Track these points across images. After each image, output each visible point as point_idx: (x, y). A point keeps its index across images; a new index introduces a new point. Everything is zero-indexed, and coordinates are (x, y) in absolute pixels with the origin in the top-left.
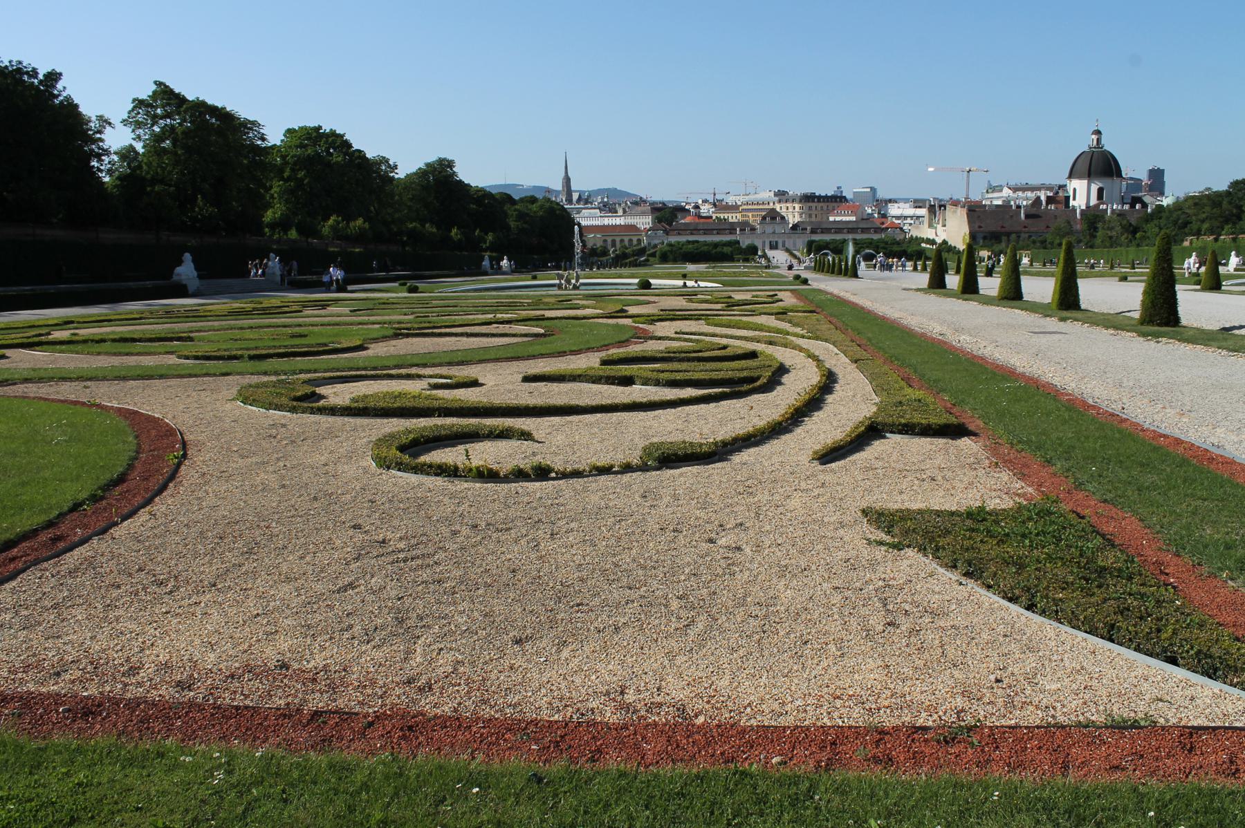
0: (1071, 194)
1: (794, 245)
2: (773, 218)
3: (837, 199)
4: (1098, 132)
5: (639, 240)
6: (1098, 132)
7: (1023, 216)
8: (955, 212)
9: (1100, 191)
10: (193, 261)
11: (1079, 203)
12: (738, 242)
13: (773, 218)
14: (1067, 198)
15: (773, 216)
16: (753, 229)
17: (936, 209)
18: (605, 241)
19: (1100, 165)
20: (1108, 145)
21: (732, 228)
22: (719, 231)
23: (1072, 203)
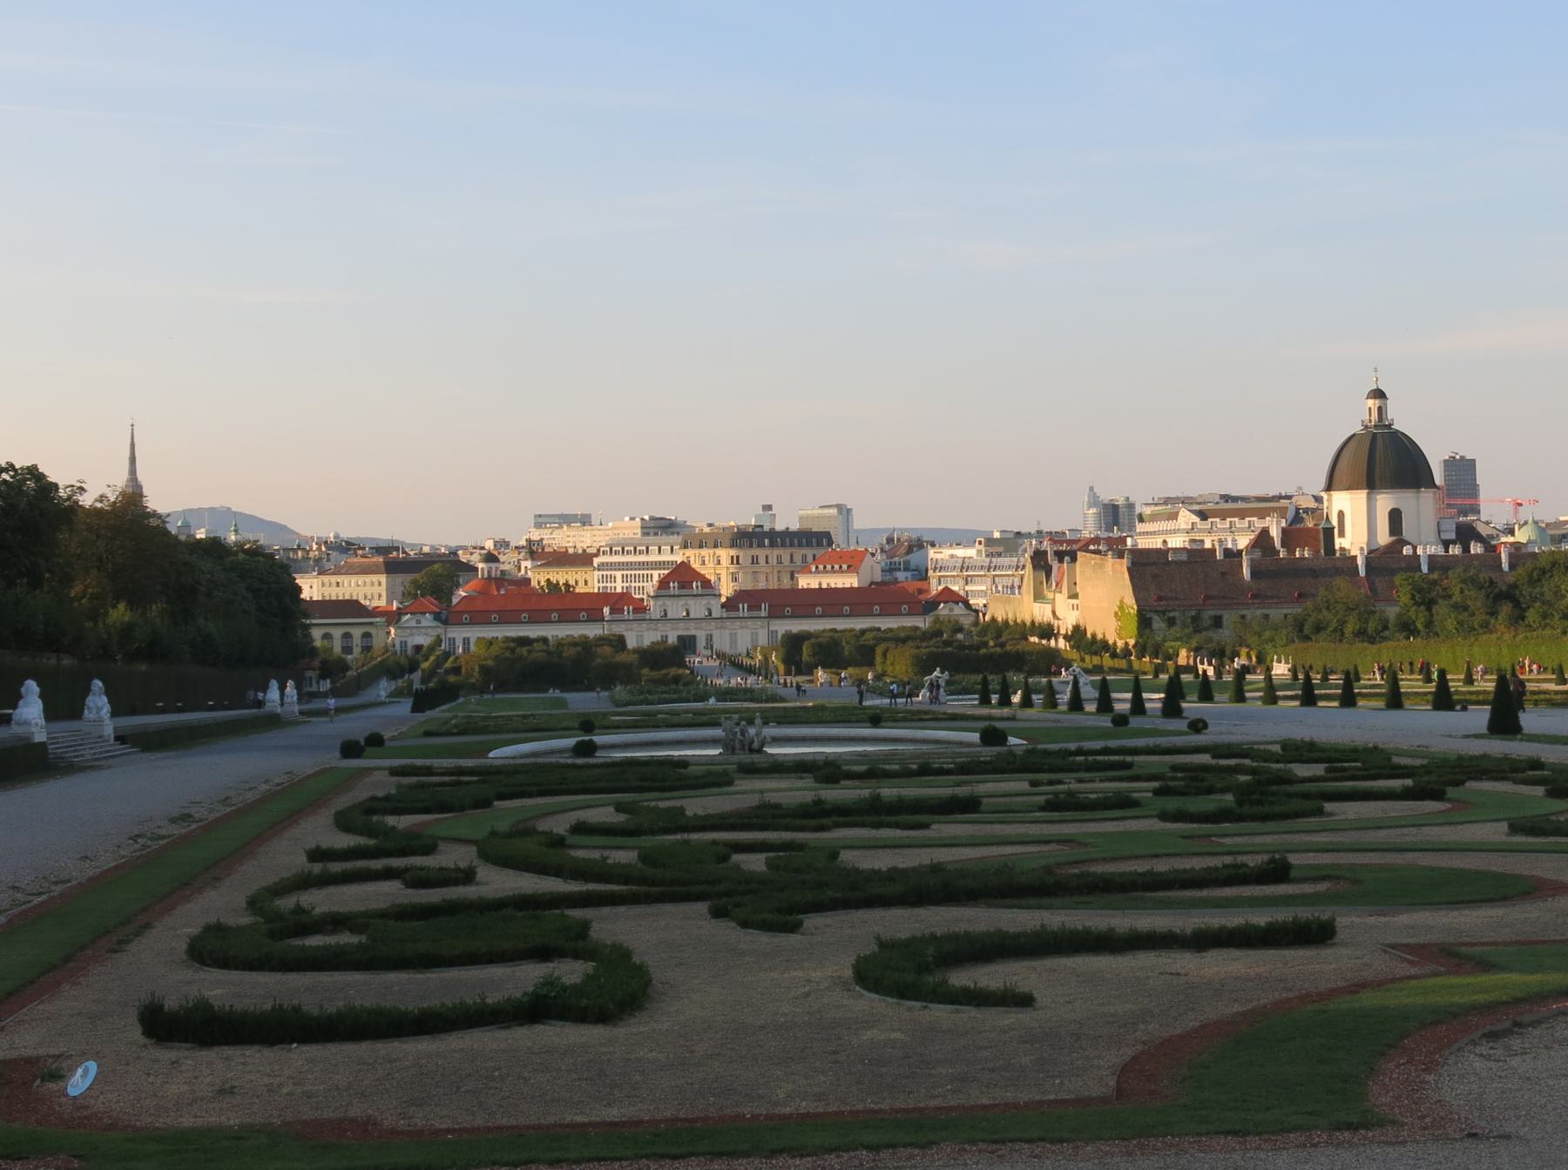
0: (1335, 522)
1: (733, 641)
3: (811, 541)
4: (1379, 394)
5: (367, 635)
6: (1379, 394)
7: (1246, 572)
8: (1101, 566)
9: (1395, 517)
10: (41, 696)
11: (1353, 541)
12: (620, 642)
14: (1329, 532)
15: (682, 578)
16: (640, 608)
17: (1052, 557)
19: (1386, 459)
20: (1402, 421)
21: (591, 607)
22: (568, 616)
23: (1339, 542)
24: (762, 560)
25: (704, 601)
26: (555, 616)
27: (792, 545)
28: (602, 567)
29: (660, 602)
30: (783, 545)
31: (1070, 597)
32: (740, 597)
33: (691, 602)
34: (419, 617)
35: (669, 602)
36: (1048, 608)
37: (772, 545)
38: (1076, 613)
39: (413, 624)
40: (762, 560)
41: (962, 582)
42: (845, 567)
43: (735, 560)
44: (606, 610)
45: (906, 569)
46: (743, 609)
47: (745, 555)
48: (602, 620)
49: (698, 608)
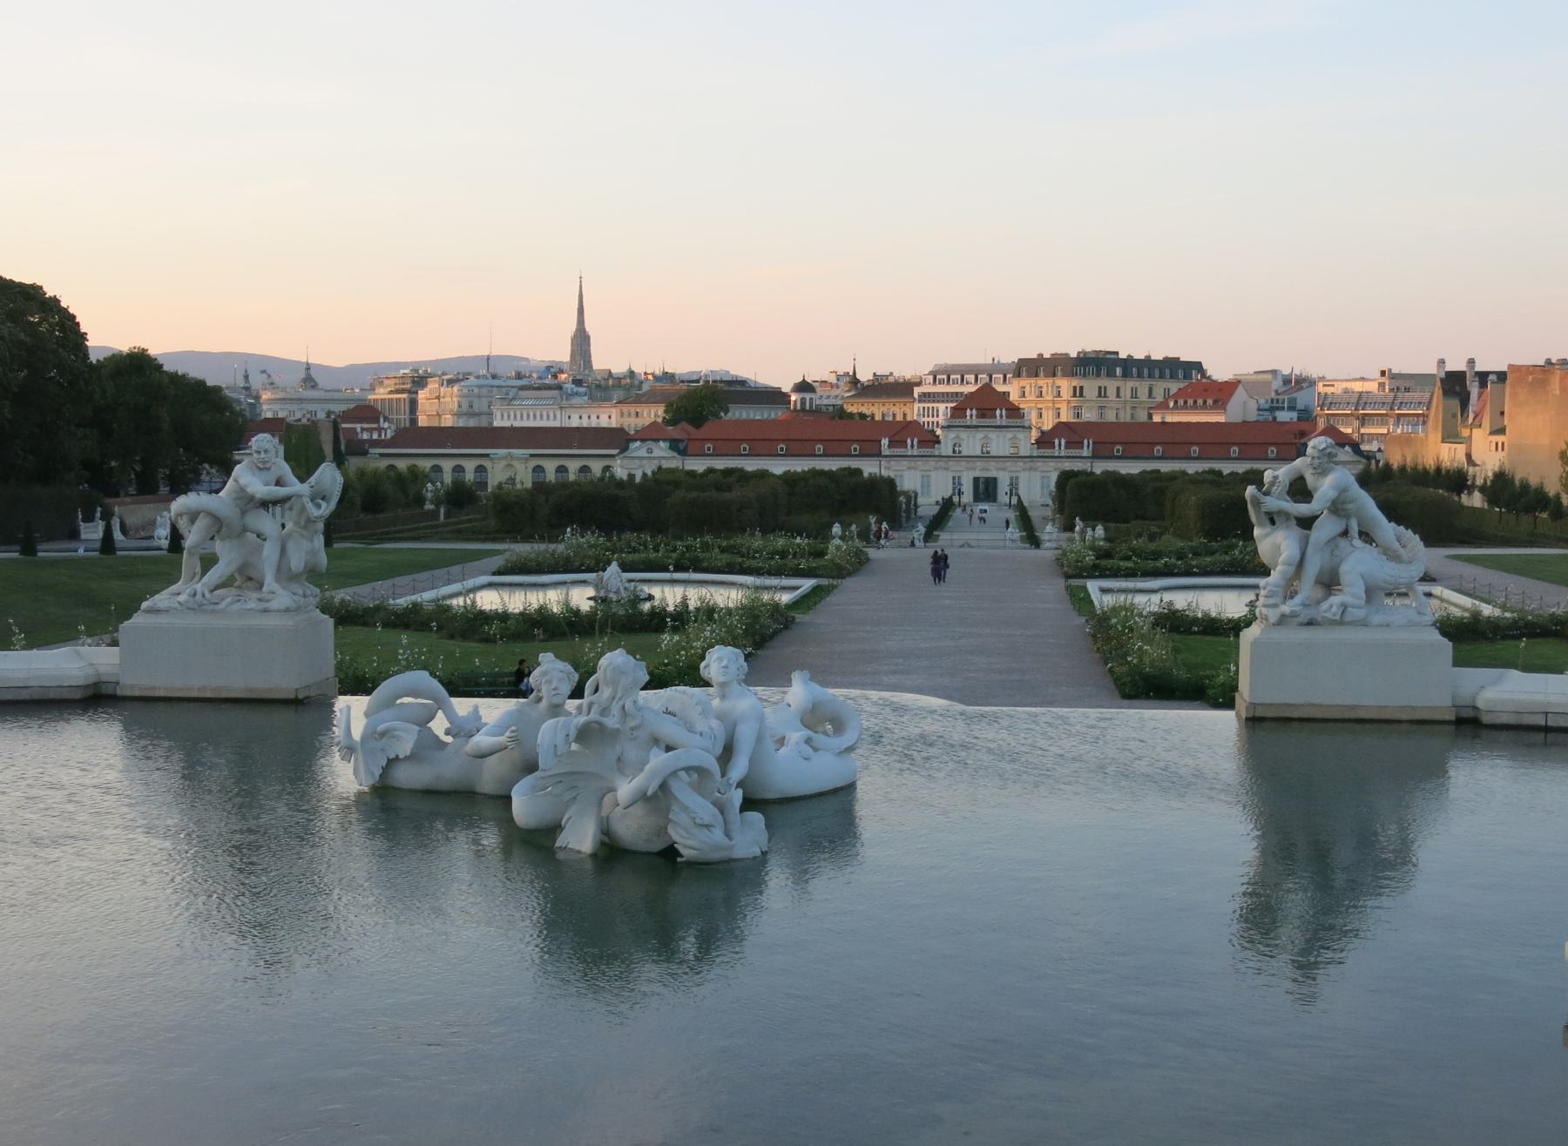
2: (986, 412)
13: (986, 412)
16: (930, 440)
18: (539, 469)
24: (1112, 393)
25: (1010, 435)
26: (819, 448)
27: (1151, 376)
28: (925, 397)
29: (952, 435)
30: (1140, 375)
31: (1492, 433)
32: (1061, 428)
33: (993, 435)
35: (964, 434)
36: (1461, 450)
37: (1126, 375)
38: (1501, 455)
39: (643, 453)
40: (1112, 393)
41: (1356, 423)
42: (1210, 402)
43: (1078, 392)
44: (885, 442)
45: (1292, 408)
46: (1060, 443)
47: (1091, 386)
48: (879, 455)
49: (1000, 443)
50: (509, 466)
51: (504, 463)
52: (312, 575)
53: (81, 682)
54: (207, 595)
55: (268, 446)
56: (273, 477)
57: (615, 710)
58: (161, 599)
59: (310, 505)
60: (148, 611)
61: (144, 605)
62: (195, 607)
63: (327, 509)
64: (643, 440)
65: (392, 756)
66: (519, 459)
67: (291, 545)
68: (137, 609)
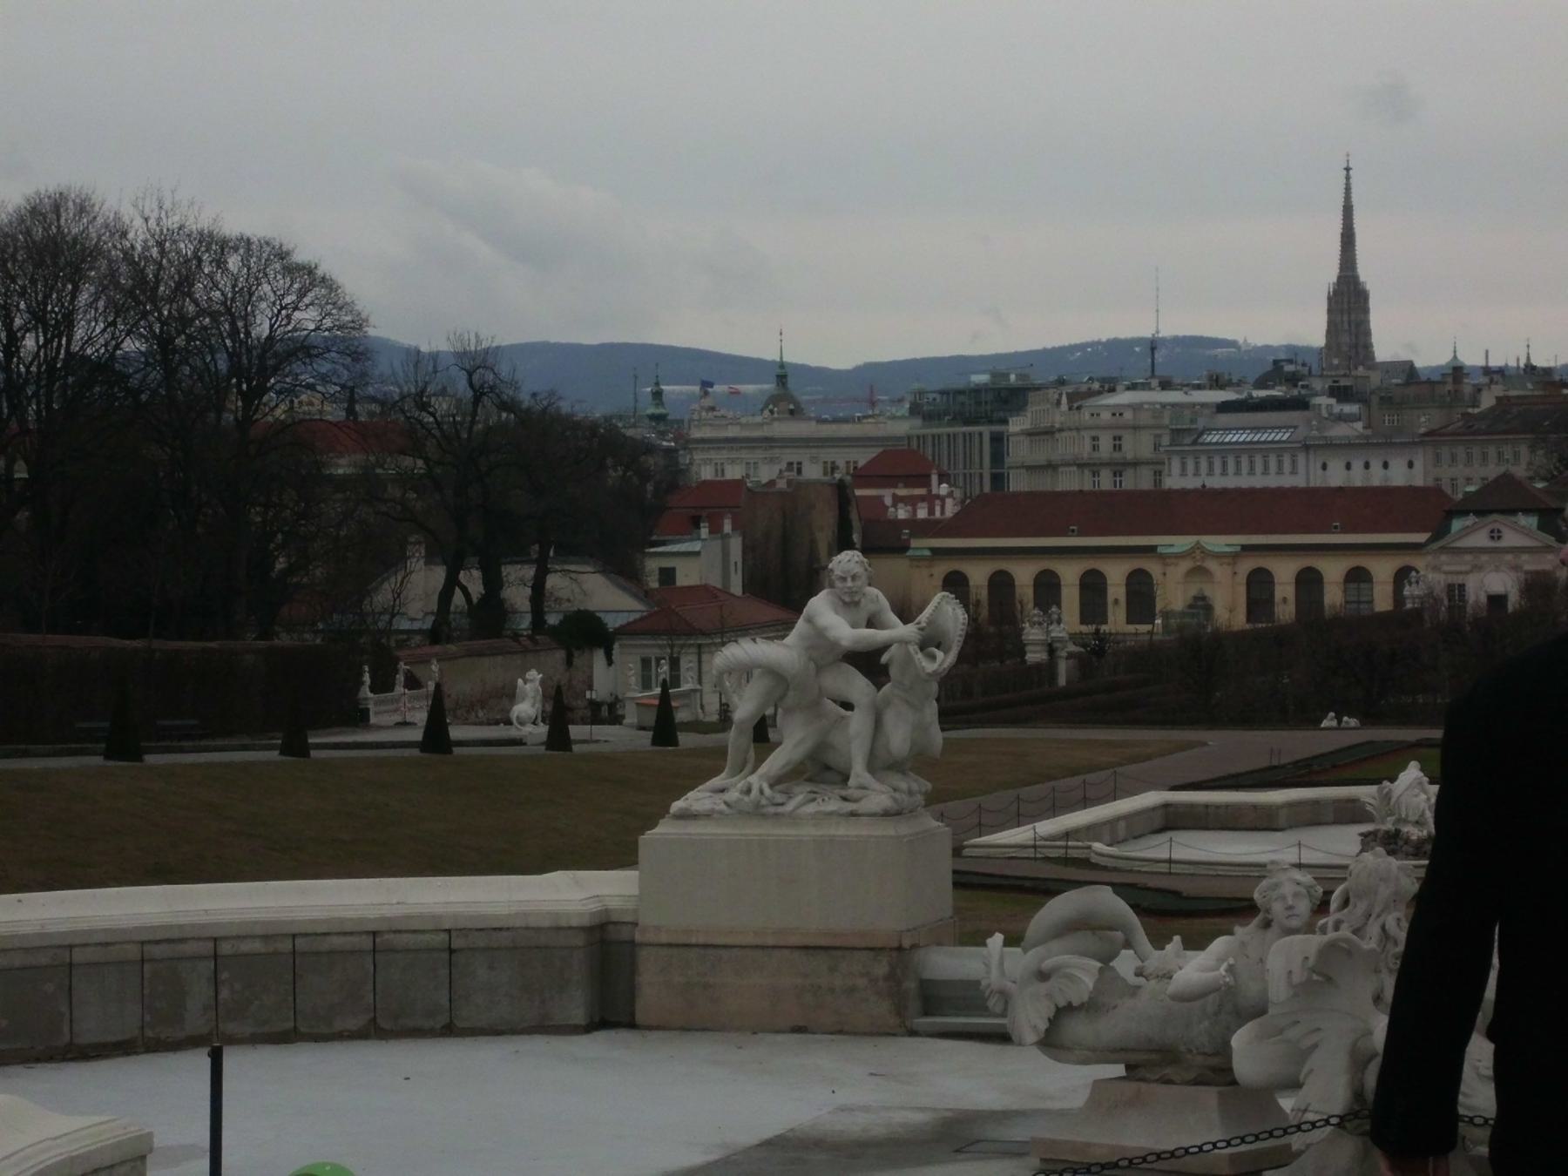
34: (1496, 521)
39: (1480, 539)
50: (1199, 571)
51: (1185, 565)
52: (919, 762)
53: (586, 922)
54: (767, 791)
55: (858, 569)
56: (863, 616)
57: (1374, 929)
58: (697, 799)
59: (919, 657)
60: (686, 816)
61: (677, 806)
62: (757, 812)
63: (944, 660)
64: (1480, 513)
65: (1062, 1003)
66: (1218, 556)
67: (889, 718)
68: (664, 811)
